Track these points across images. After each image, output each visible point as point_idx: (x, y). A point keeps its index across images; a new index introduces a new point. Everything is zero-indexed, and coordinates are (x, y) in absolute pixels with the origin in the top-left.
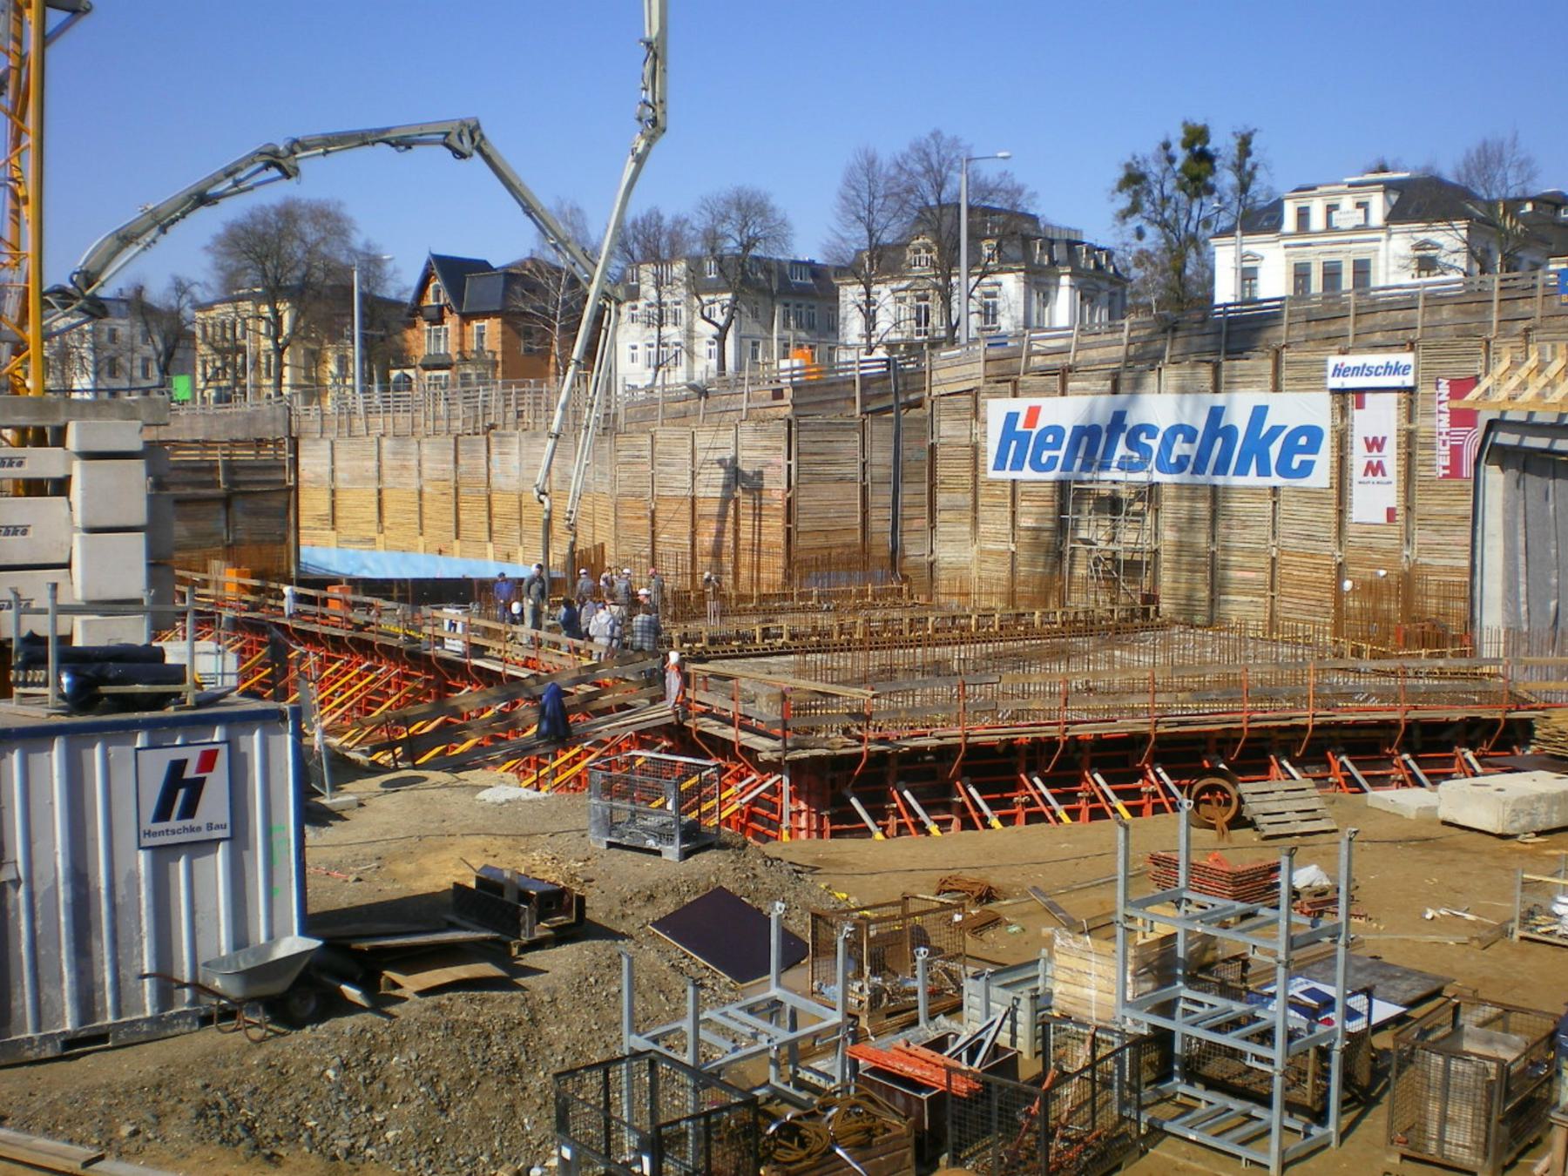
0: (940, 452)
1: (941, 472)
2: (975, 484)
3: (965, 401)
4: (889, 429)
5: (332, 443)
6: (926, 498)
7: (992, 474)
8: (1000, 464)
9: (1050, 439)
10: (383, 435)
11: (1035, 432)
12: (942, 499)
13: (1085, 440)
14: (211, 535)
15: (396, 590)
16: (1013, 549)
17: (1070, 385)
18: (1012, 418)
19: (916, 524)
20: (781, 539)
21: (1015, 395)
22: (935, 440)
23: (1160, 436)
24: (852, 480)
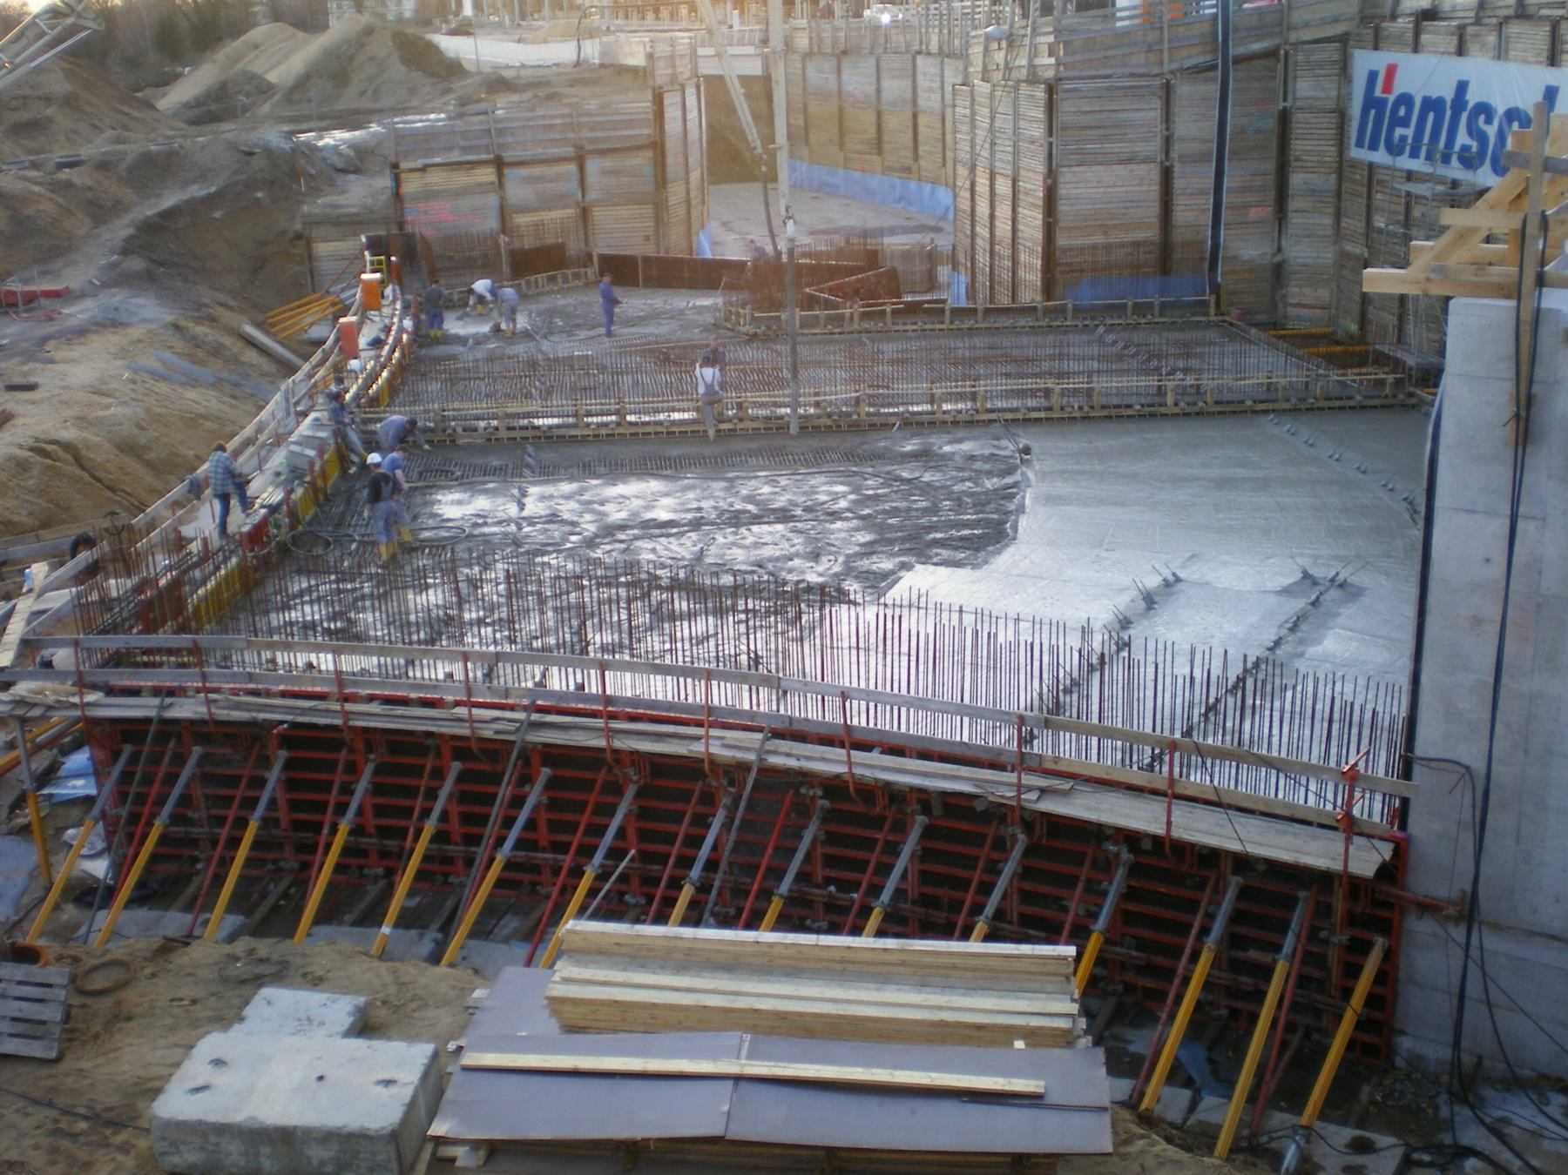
0: (1298, 118)
1: (1298, 146)
2: (1340, 162)
3: (1332, 52)
4: (1214, 89)
5: (878, 60)
6: (1270, 180)
7: (1356, 153)
8: (1360, 144)
9: (1402, 112)
10: (919, 53)
11: (1391, 98)
12: (1297, 180)
13: (1431, 116)
14: (562, 196)
15: (686, 270)
16: (1366, 255)
17: (1424, 38)
18: (1373, 76)
19: (1253, 214)
20: (1038, 235)
21: (1376, 48)
22: (1288, 104)
23: (1496, 123)
24: (1146, 160)
